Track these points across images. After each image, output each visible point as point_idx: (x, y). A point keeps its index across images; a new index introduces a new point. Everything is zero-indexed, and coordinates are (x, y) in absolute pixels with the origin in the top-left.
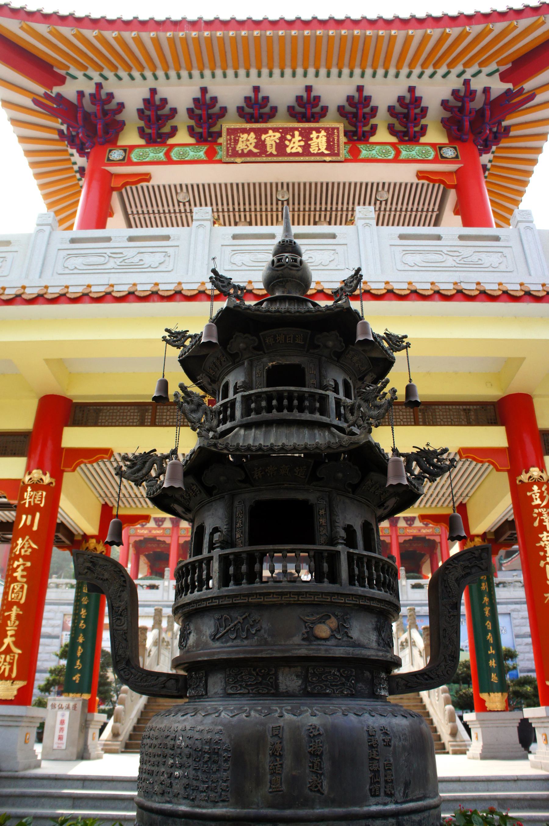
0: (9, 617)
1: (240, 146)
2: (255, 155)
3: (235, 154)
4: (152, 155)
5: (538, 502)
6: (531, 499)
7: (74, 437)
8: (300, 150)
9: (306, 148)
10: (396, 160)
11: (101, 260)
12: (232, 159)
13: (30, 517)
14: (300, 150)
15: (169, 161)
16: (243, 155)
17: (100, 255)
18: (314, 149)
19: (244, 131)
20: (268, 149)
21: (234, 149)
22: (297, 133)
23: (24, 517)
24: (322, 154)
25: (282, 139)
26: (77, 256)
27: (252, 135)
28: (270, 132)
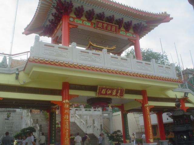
0: (66, 132)
1: (99, 26)
2: (101, 28)
3: (98, 27)
4: (79, 22)
5: (148, 110)
6: (147, 109)
7: (72, 92)
8: (110, 29)
9: (111, 29)
10: (126, 35)
11: (88, 58)
12: (97, 28)
13: (67, 111)
14: (110, 29)
15: (83, 25)
16: (99, 28)
17: (88, 56)
18: (112, 30)
19: (100, 22)
20: (104, 28)
21: (97, 26)
22: (110, 25)
23: (66, 110)
24: (114, 31)
25: (107, 26)
26: (83, 56)
27: (102, 23)
28: (105, 24)
